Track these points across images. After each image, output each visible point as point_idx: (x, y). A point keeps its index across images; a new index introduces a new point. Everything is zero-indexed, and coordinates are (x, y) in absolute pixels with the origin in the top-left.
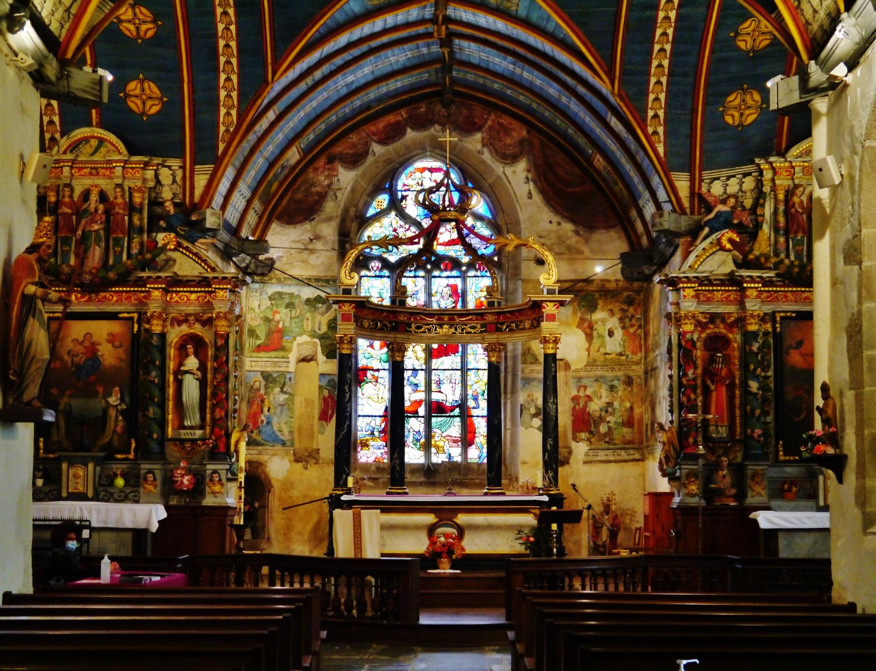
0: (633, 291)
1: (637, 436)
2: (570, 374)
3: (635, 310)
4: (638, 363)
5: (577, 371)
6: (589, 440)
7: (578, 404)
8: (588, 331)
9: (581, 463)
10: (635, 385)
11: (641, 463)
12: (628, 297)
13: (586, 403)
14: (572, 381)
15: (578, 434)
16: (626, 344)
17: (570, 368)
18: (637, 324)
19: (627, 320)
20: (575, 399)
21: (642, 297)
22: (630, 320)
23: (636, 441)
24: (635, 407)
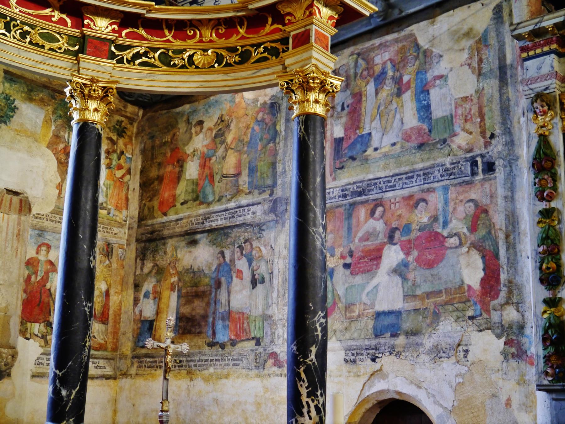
0: (126, 117)
1: (110, 339)
2: (28, 220)
3: (126, 145)
4: (121, 225)
5: (39, 217)
6: (44, 337)
7: (36, 273)
8: (63, 157)
9: (29, 377)
10: (114, 259)
11: (111, 382)
12: (119, 123)
13: (47, 273)
14: (30, 232)
15: (29, 324)
16: (110, 192)
17: (30, 210)
18: (126, 166)
19: (115, 156)
20: (31, 263)
21: (135, 130)
22: (119, 159)
23: (109, 346)
24: (112, 292)
